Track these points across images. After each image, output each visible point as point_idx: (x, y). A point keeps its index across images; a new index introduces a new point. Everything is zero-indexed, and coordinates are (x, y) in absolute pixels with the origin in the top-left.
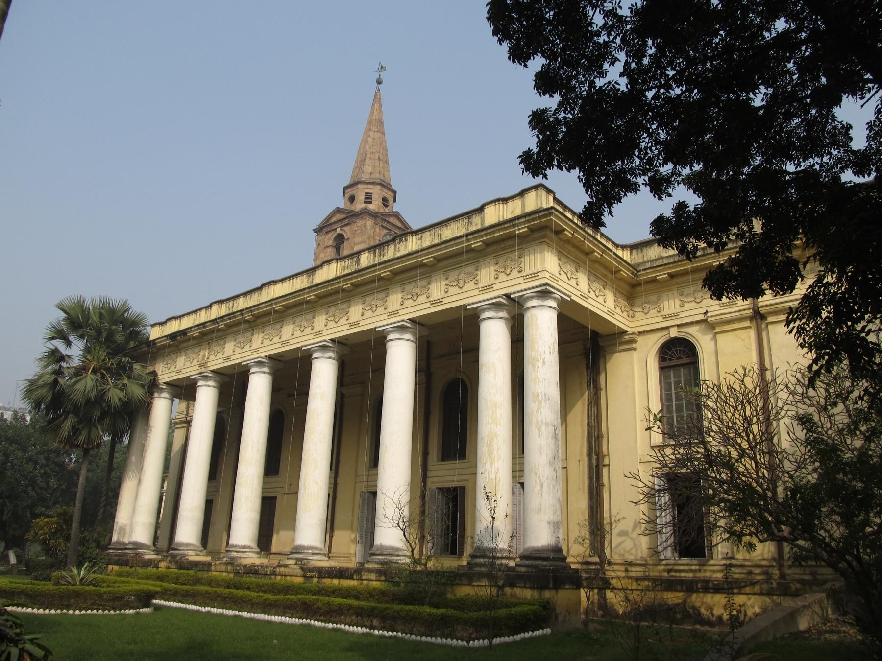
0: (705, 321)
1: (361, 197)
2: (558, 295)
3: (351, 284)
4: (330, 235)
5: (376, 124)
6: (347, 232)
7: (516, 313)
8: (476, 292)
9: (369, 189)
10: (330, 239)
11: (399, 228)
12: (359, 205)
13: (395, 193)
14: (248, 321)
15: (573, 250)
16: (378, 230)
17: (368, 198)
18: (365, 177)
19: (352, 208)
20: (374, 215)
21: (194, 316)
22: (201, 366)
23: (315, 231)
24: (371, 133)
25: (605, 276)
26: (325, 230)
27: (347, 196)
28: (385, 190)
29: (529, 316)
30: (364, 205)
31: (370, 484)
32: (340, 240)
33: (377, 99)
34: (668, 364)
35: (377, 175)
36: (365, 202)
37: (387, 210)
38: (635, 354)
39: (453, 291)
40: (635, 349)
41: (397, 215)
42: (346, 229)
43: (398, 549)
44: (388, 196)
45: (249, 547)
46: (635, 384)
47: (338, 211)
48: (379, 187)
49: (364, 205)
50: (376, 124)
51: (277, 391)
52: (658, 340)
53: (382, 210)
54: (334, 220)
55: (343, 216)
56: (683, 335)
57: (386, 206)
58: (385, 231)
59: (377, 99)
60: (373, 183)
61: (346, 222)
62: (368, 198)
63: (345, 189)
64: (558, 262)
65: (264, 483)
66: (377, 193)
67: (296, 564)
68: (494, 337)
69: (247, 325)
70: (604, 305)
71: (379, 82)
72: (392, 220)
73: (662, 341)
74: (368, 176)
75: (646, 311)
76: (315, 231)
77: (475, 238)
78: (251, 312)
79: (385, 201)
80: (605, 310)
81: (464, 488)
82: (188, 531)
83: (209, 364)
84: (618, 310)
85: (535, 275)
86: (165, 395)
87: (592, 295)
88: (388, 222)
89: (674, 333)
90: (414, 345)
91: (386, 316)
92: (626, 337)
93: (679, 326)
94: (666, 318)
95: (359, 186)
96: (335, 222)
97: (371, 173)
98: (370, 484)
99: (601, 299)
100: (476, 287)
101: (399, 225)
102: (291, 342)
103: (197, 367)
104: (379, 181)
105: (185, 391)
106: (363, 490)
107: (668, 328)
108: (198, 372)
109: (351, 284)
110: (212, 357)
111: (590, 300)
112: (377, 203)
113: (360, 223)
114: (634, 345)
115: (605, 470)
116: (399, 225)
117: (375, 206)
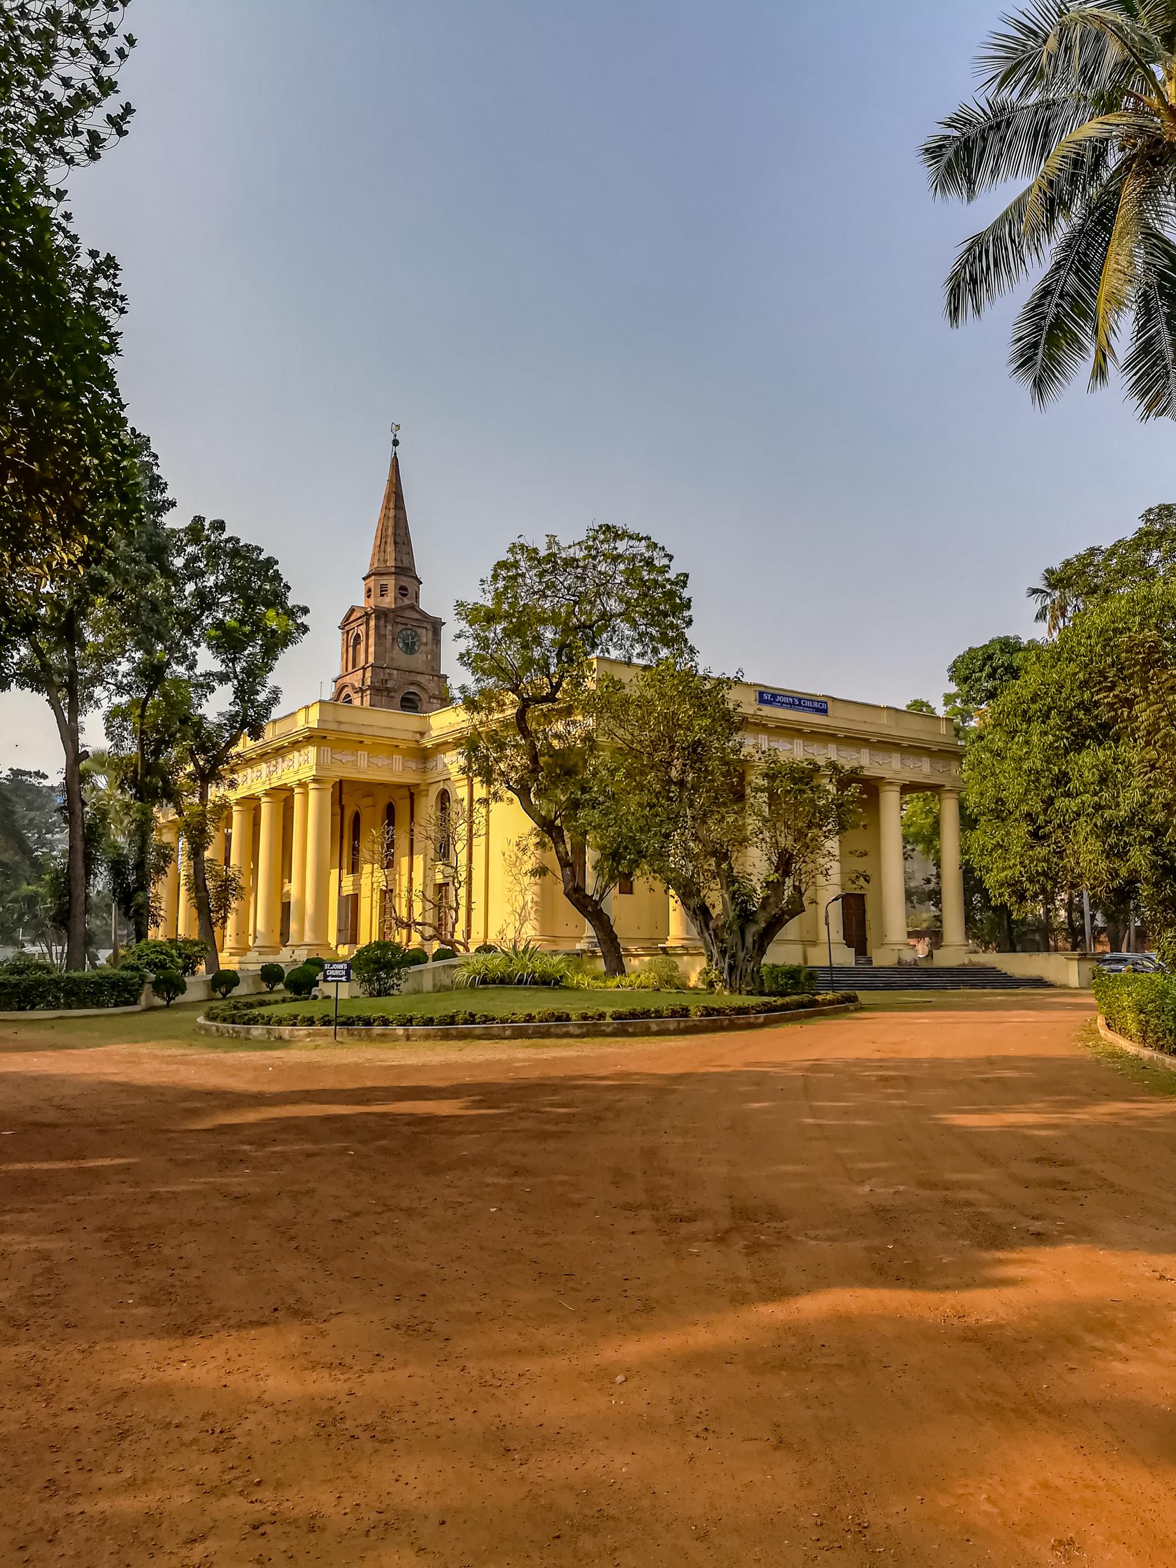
1: (376, 591)
9: (384, 580)
36: (382, 595)
53: (400, 603)
54: (352, 619)
57: (405, 595)
58: (401, 627)
71: (396, 443)
72: (409, 614)
92: (422, 788)
101: (417, 616)
116: (417, 616)
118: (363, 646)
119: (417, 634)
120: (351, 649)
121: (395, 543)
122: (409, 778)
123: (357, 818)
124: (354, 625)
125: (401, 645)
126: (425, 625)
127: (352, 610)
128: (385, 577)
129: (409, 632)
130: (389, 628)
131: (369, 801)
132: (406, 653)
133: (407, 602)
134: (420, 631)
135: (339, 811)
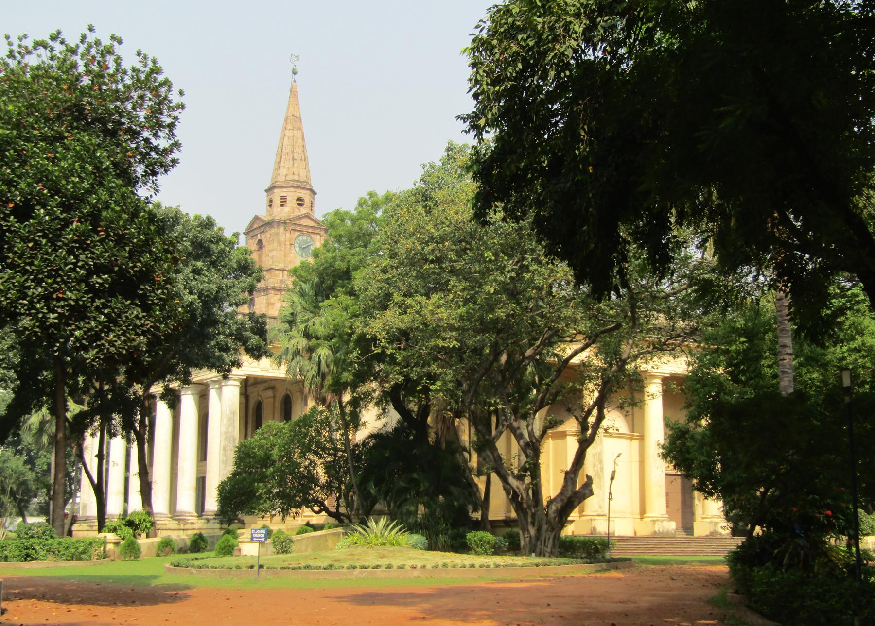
1: (277, 202)
5: (294, 121)
6: (265, 237)
9: (284, 192)
16: (288, 235)
17: (283, 200)
18: (281, 179)
24: (287, 132)
33: (294, 93)
35: (290, 178)
36: (282, 206)
48: (292, 189)
50: (294, 121)
54: (255, 226)
57: (301, 205)
58: (297, 233)
59: (294, 93)
61: (262, 229)
62: (283, 200)
65: (198, 467)
66: (292, 195)
71: (295, 73)
72: (304, 222)
74: (284, 179)
79: (300, 201)
95: (275, 190)
113: (273, 231)
121: (293, 159)
123: (259, 407)
125: (298, 249)
126: (319, 231)
127: (256, 218)
129: (305, 238)
131: (270, 393)
133: (303, 211)
134: (314, 236)
135: (244, 401)
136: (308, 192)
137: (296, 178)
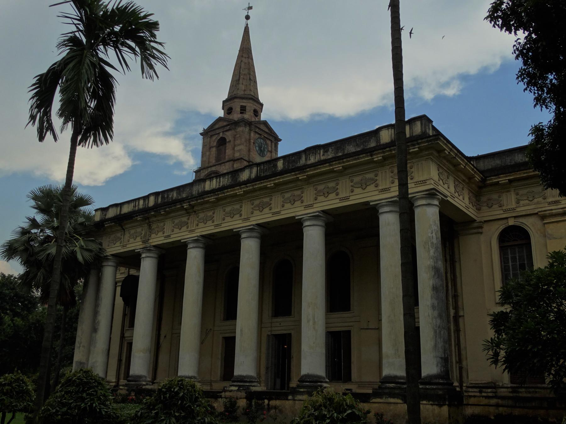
0: (537, 214)
2: (440, 196)
3: (274, 184)
4: (214, 138)
5: (246, 51)
6: (229, 136)
7: (406, 210)
8: (377, 193)
10: (214, 141)
11: (267, 133)
12: (236, 116)
13: (262, 105)
14: (186, 209)
15: (447, 163)
16: (252, 134)
17: (243, 109)
18: (240, 93)
19: (231, 117)
20: (249, 124)
21: (132, 204)
22: (144, 242)
23: (201, 134)
25: (464, 181)
26: (210, 134)
27: (226, 108)
28: (255, 103)
29: (418, 212)
30: (240, 116)
31: (273, 329)
32: (222, 142)
34: (507, 244)
36: (241, 113)
37: (257, 120)
38: (482, 238)
39: (357, 191)
40: (481, 233)
41: (265, 123)
42: (229, 133)
43: (320, 377)
44: (258, 109)
45: (195, 377)
46: (483, 259)
47: (220, 119)
48: (251, 101)
49: (240, 116)
50: (246, 51)
51: (209, 260)
52: (499, 227)
53: (253, 119)
54: (217, 126)
55: (225, 124)
56: (518, 224)
58: (257, 136)
60: (246, 98)
62: (243, 109)
63: (224, 102)
64: (438, 172)
66: (250, 106)
67: (238, 390)
68: (389, 225)
69: (184, 212)
70: (462, 202)
71: (248, 17)
73: (502, 228)
75: (490, 206)
76: (201, 134)
77: (377, 154)
78: (189, 202)
80: (464, 205)
81: (349, 332)
82: (139, 366)
83: (151, 241)
84: (471, 206)
85: (424, 182)
86: (110, 263)
87: (457, 194)
88: (259, 128)
89: (511, 222)
90: (323, 229)
91: (303, 208)
92: (475, 225)
93: (515, 217)
94: (505, 211)
95: (236, 100)
96: (218, 128)
97: (245, 90)
98: (273, 329)
99: (461, 198)
100: (376, 189)
101: (267, 131)
102: (223, 225)
103: (141, 243)
104: (251, 97)
105: (132, 260)
106: (269, 333)
107: (507, 218)
108: (141, 247)
109: (274, 184)
110: (153, 236)
111: (456, 199)
112: (249, 113)
113: (240, 129)
114: (480, 230)
115: (461, 320)
116: (267, 131)
117: (248, 116)
118: (229, 147)
119: (267, 144)
120: (214, 149)
122: (471, 212)
124: (217, 132)
125: (257, 148)
126: (271, 138)
128: (244, 101)
129: (262, 141)
130: (252, 134)
132: (260, 155)
136: (260, 106)
137: (252, 94)
